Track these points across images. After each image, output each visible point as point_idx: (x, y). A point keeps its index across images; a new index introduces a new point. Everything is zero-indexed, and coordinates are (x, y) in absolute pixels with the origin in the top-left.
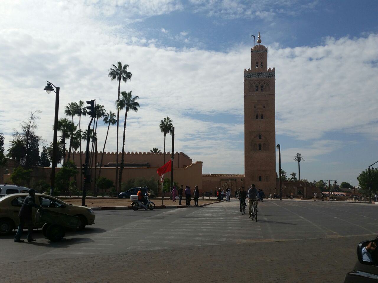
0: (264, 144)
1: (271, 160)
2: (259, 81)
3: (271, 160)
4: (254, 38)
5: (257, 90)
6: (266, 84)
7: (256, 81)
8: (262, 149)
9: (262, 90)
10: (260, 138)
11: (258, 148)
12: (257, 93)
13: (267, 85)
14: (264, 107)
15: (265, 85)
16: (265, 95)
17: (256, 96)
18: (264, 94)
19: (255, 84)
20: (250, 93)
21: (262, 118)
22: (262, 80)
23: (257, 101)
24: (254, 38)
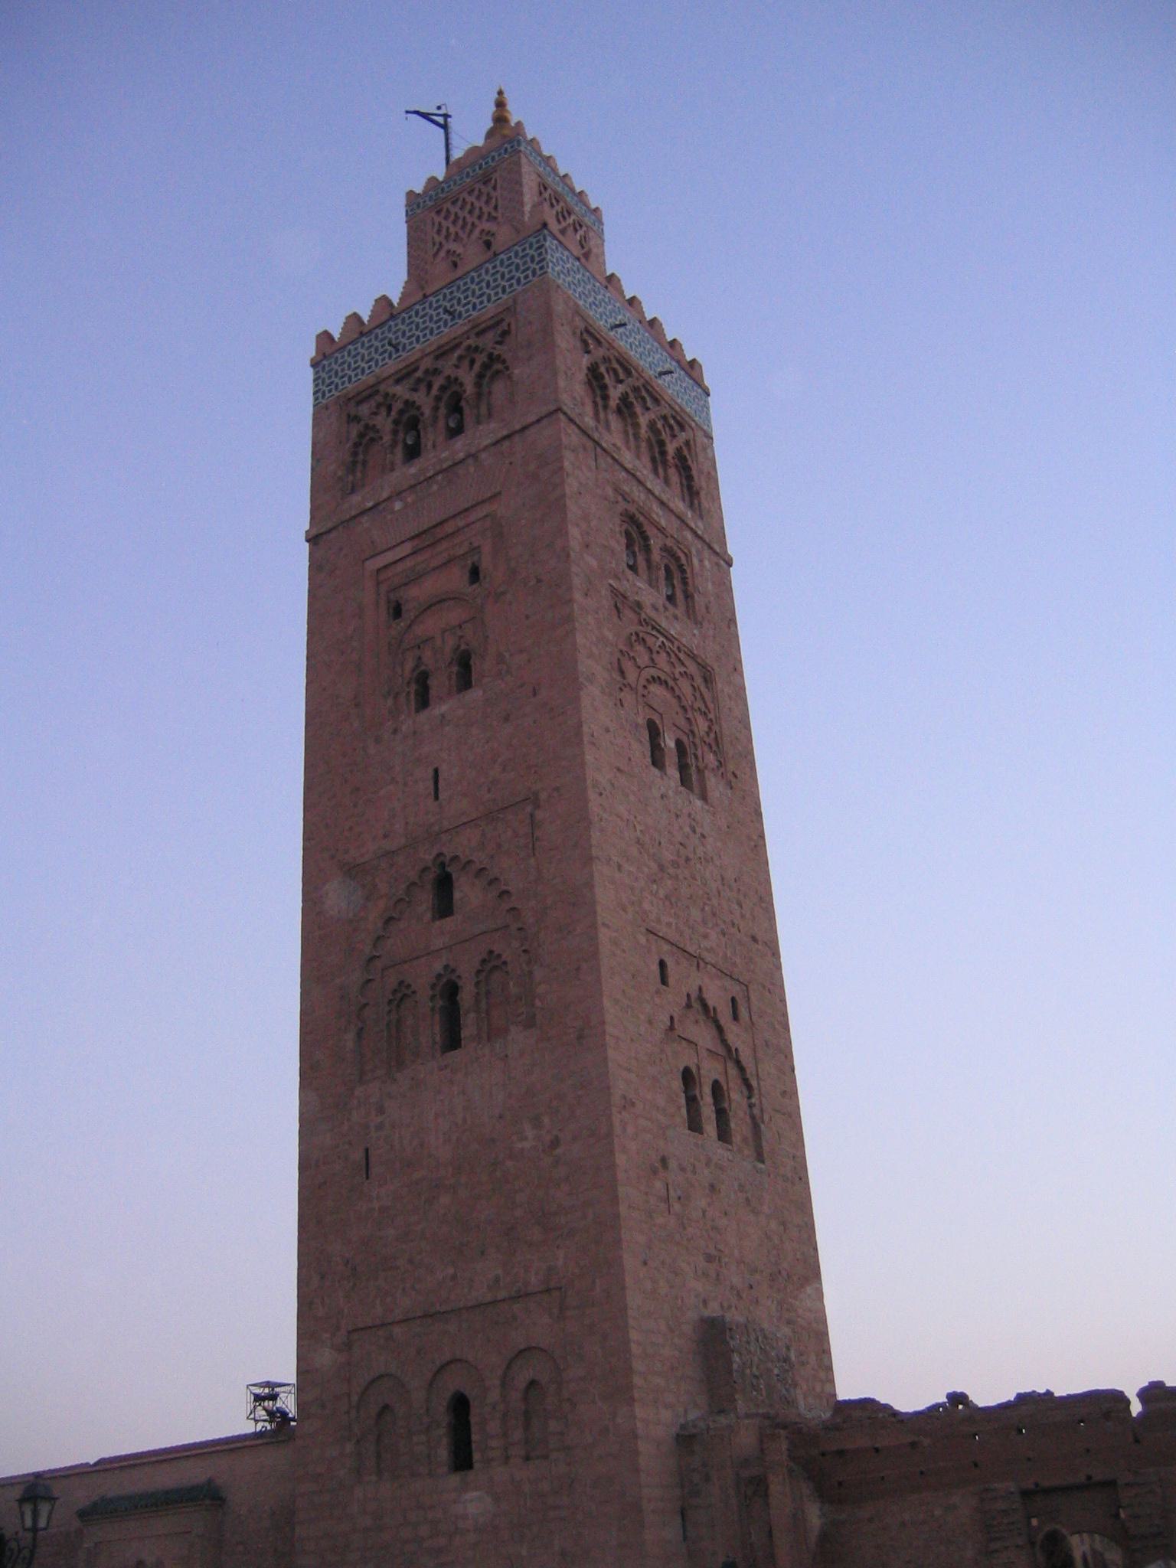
0: (491, 964)
1: (555, 1143)
2: (419, 374)
3: (555, 1143)
4: (445, 127)
5: (413, 452)
6: (477, 367)
7: (398, 381)
8: (469, 1027)
9: (456, 432)
10: (444, 906)
11: (431, 1031)
12: (413, 470)
13: (486, 367)
14: (475, 574)
15: (468, 379)
16: (473, 456)
17: (398, 506)
18: (461, 455)
19: (398, 406)
20: (356, 499)
21: (465, 682)
22: (442, 353)
23: (407, 548)
24: (445, 127)
